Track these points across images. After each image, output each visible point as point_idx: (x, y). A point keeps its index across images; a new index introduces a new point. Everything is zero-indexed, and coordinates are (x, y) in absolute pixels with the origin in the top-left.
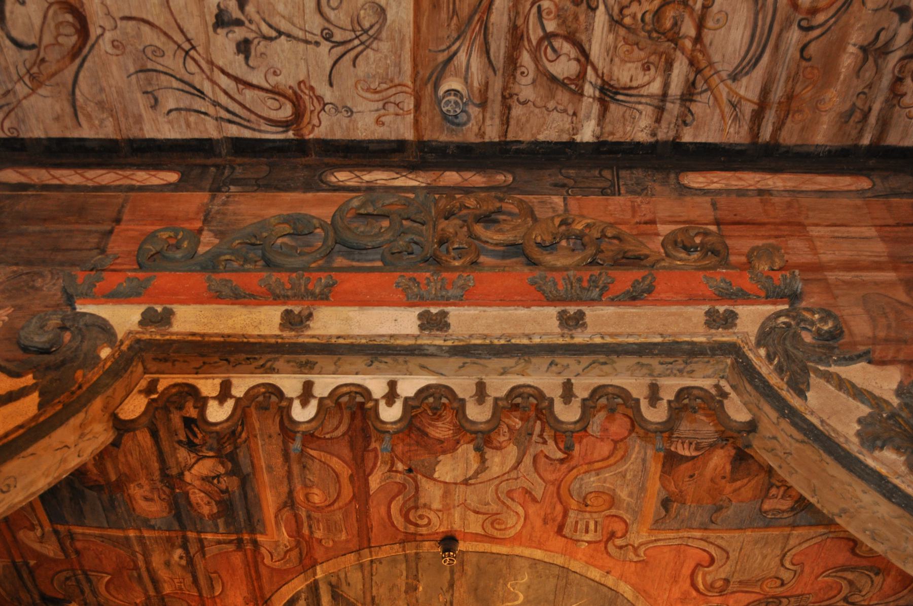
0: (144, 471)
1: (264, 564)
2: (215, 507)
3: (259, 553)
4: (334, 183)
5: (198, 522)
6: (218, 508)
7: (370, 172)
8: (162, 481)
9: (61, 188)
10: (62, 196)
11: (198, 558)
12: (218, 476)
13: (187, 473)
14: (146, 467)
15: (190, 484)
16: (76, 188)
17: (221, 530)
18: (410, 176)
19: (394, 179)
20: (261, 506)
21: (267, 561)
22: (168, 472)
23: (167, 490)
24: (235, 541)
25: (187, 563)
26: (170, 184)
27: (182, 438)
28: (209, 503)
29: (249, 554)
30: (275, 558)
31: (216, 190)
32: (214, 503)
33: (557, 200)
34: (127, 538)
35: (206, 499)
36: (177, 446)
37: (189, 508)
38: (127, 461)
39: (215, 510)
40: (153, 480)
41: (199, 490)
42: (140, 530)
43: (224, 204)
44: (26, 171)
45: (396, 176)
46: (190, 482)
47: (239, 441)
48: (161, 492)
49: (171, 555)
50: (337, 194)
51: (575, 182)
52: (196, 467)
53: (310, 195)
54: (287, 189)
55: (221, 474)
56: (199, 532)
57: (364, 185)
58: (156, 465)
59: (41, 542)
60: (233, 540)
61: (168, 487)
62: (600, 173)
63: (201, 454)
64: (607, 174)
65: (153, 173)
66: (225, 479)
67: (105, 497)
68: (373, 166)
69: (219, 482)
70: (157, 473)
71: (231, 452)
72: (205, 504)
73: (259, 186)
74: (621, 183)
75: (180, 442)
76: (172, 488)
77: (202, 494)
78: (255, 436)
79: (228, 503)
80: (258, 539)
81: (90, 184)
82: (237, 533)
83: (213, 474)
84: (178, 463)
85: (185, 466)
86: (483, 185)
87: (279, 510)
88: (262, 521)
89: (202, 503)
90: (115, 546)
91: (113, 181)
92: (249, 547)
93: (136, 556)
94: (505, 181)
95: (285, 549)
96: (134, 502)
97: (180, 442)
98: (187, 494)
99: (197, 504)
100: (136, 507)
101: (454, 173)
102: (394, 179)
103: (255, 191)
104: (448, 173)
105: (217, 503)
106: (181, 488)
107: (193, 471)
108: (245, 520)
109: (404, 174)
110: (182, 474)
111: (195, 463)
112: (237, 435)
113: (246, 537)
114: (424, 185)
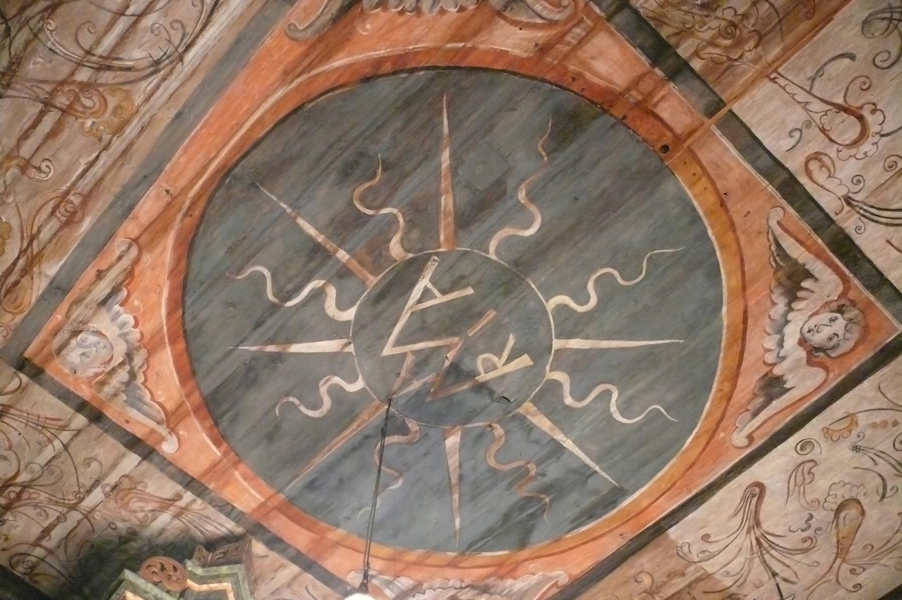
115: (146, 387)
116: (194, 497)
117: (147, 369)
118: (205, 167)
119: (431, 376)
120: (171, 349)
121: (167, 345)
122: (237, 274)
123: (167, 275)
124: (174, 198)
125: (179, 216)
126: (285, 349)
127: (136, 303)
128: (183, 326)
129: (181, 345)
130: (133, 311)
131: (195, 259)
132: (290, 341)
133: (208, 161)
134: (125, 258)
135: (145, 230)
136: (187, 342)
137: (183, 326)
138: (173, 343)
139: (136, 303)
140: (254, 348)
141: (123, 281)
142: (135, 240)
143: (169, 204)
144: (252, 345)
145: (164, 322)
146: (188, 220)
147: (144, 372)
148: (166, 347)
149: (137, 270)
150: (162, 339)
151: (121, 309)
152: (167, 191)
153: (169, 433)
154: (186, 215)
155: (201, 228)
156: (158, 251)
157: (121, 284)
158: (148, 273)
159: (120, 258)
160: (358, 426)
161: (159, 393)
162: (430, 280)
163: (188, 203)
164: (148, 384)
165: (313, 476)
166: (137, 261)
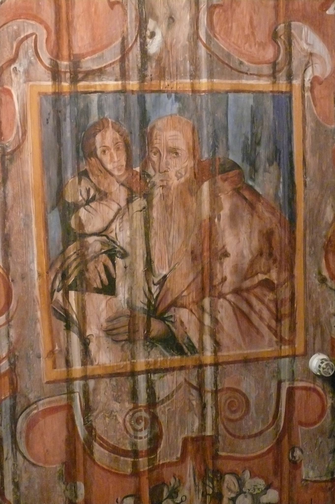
0: (169, 203)
1: (47, 28)
2: (98, 145)
3: (51, 53)
5: (122, 115)
6: (94, 143)
8: (154, 185)
11: (132, 33)
12: (88, 202)
13: (123, 203)
14: (167, 208)
15: (122, 184)
17: (95, 97)
20: (42, 150)
21: (42, 34)
22: (144, 202)
23: (151, 171)
24: (80, 76)
25: (146, 22)
27: (119, 262)
28: (104, 152)
29: (65, 52)
30: (30, 42)
32: (99, 152)
34: (211, 76)
35: (106, 159)
36: (128, 249)
37: (129, 138)
38: (186, 217)
39: (98, 138)
40: (163, 187)
41: (112, 175)
42: (194, 91)
46: (122, 187)
47: (58, 265)
48: (157, 167)
49: (165, 42)
52: (111, 215)
55: (84, 206)
56: (123, 91)
58: (155, 214)
59: (311, 54)
60: (83, 79)
61: (149, 176)
63: (105, 238)
66: (80, 198)
67: (221, 153)
69: (88, 191)
70: (156, 201)
71: (69, 245)
72: (108, 148)
75: (124, 255)
76: (144, 174)
77: (109, 167)
78: (40, 275)
79: (81, 154)
80: (50, 83)
82: (77, 92)
83: (93, 205)
84: (131, 220)
85: (124, 214)
87: (19, 148)
88: (43, 122)
89: (112, 151)
90: (229, 55)
92: (64, 64)
93: (208, 37)
95: (16, 65)
96: (191, 144)
97: (124, 255)
98: (129, 165)
99: (118, 149)
100: (189, 134)
105: (93, 154)
106: (134, 174)
107: (115, 207)
108: (65, 120)
110: (129, 201)
111: (112, 221)
112: (60, 275)
113: (66, 85)
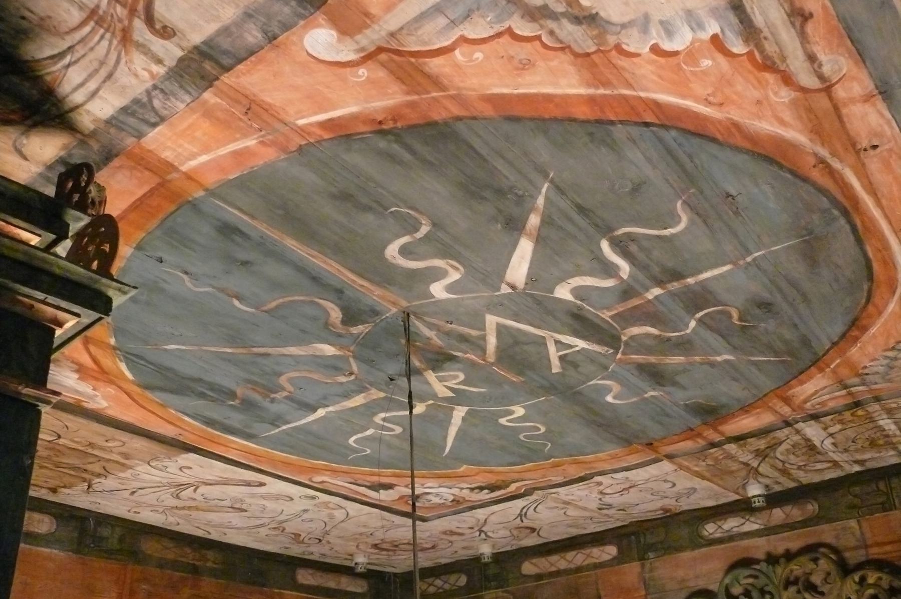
4: (706, 536)
7: (726, 519)
9: (558, 573)
10: (562, 580)
16: (567, 572)
18: (752, 519)
19: (742, 524)
26: (614, 558)
31: (642, 558)
33: (853, 523)
43: (651, 570)
44: (534, 561)
45: (743, 521)
50: (712, 547)
51: (862, 500)
53: (697, 553)
54: (680, 549)
57: (726, 535)
62: (877, 487)
64: (882, 485)
65: (601, 548)
68: (726, 513)
73: (663, 548)
74: (895, 495)
81: (572, 566)
86: (800, 519)
91: (584, 561)
94: (814, 511)
101: (778, 509)
102: (742, 524)
103: (664, 554)
104: (774, 511)
109: (747, 518)
114: (762, 527)
115: (499, 35)
116: (171, 62)
117: (545, 46)
118: (873, 192)
119: (441, 343)
120: (580, 96)
121: (591, 91)
122: (684, 202)
123: (735, 118)
124: (858, 152)
125: (824, 152)
126: (529, 236)
127: (706, 63)
128: (621, 122)
129: (582, 112)
130: (691, 54)
131: (740, 159)
132: (540, 240)
133: (879, 196)
134: (807, 64)
135: (836, 108)
136: (588, 122)
137: (621, 122)
138: (591, 100)
139: (706, 63)
140: (541, 201)
141: (762, 51)
142: (828, 89)
143: (854, 145)
144: (547, 198)
145: (643, 94)
146: (812, 161)
147: (538, 38)
148: (589, 85)
149: (770, 77)
150: (606, 84)
151: (705, 36)
152: (875, 147)
153: (362, 49)
154: (822, 161)
155: (789, 176)
156: (787, 116)
157: (759, 46)
158: (757, 94)
159: (812, 58)
160: (362, 286)
161: (479, 55)
162: (583, 349)
163: (836, 164)
164: (506, 39)
165: (252, 234)
166: (787, 79)
